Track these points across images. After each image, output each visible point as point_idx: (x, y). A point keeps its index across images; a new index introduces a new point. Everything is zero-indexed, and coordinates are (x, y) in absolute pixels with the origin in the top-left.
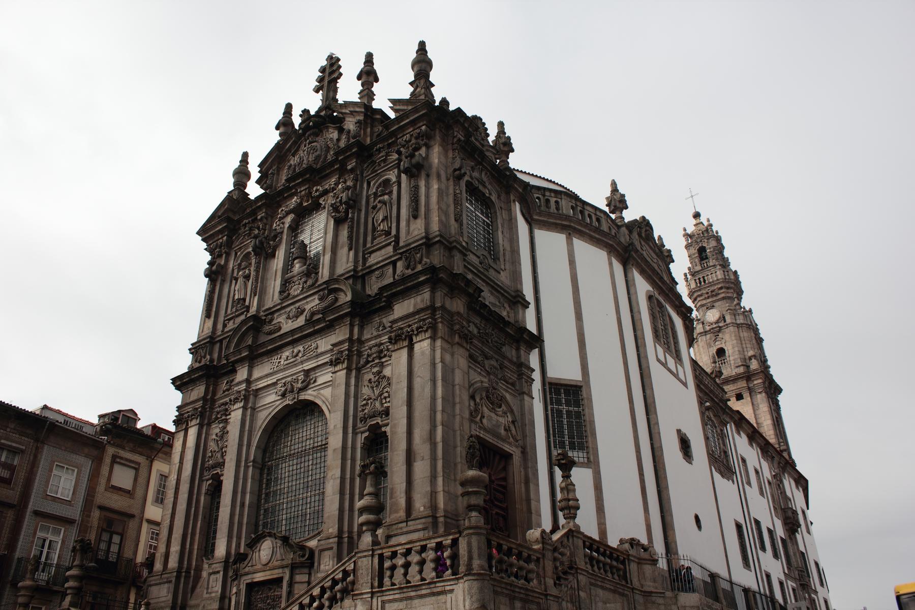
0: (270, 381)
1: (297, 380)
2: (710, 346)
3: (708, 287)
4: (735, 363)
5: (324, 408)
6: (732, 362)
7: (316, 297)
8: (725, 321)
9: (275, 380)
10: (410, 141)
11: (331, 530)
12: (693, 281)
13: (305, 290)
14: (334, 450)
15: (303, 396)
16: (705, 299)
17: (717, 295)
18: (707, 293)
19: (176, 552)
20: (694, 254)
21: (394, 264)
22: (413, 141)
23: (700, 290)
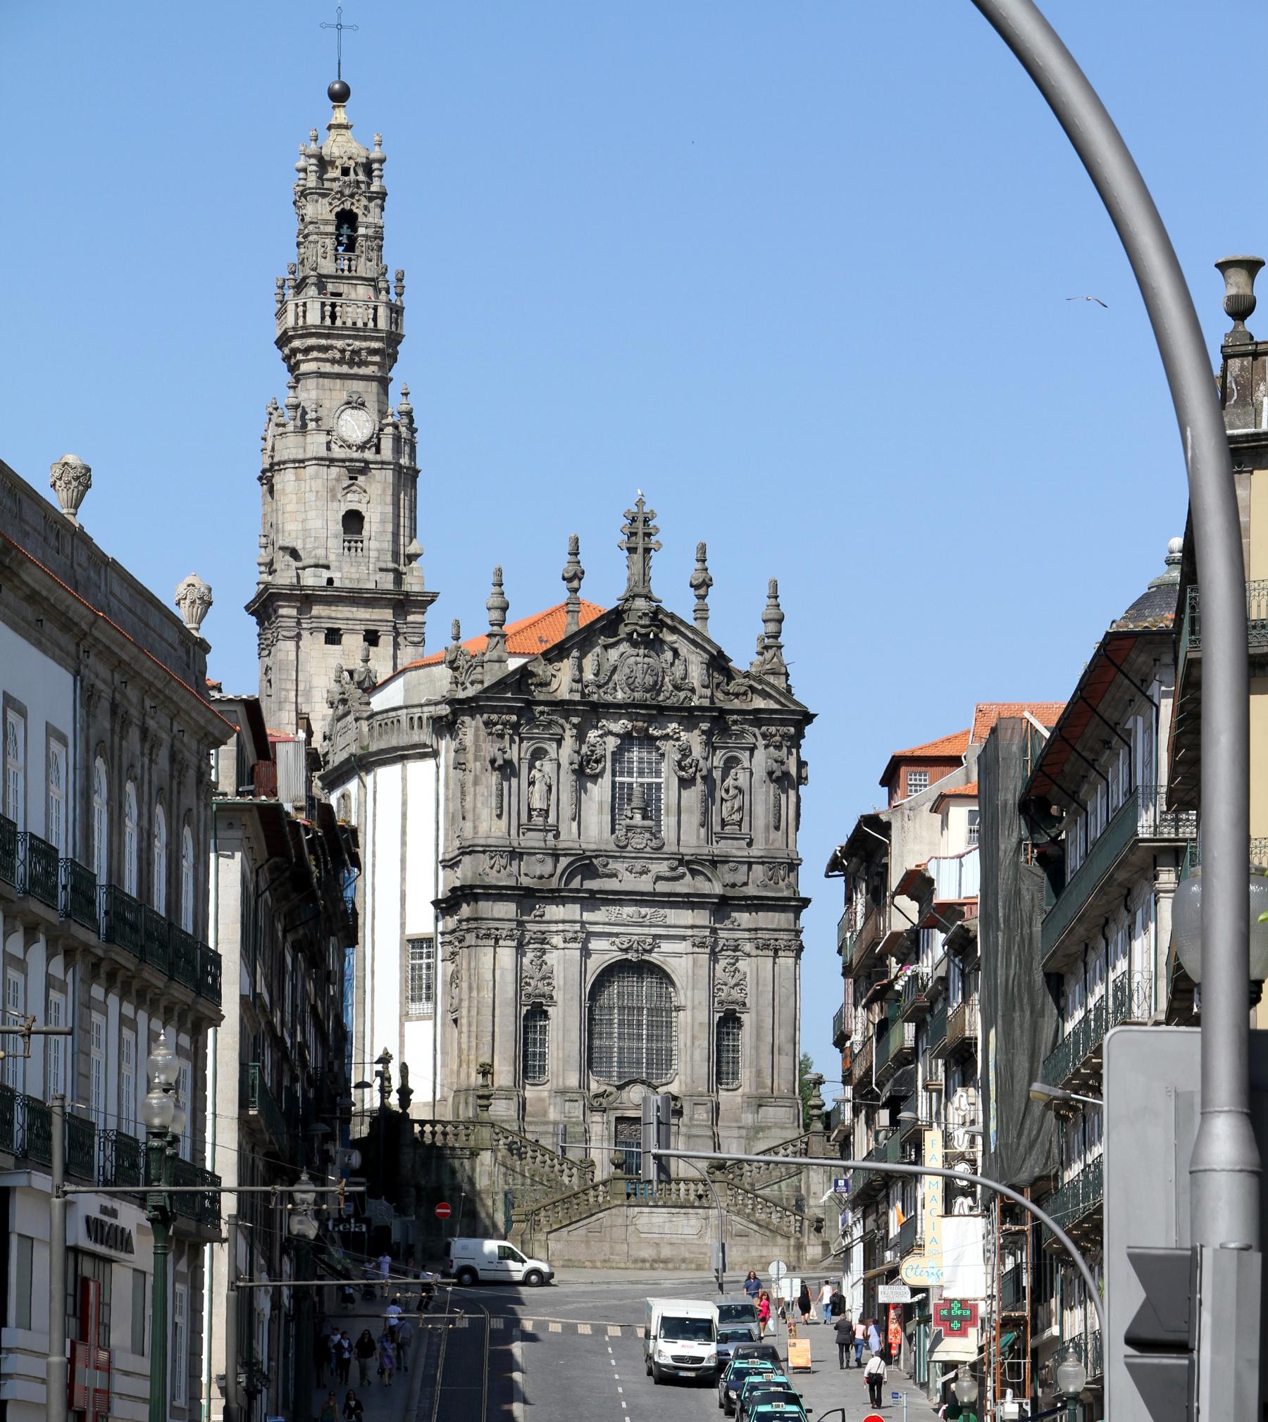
0: (607, 929)
1: (644, 942)
2: (334, 498)
3: (349, 337)
4: (378, 559)
5: (673, 976)
6: (373, 554)
7: (666, 862)
8: (378, 451)
9: (615, 931)
10: (775, 735)
11: (700, 1089)
12: (318, 306)
13: (648, 849)
14: (700, 1024)
15: (646, 957)
16: (333, 361)
17: (362, 363)
18: (343, 351)
19: (509, 1072)
20: (326, 222)
21: (750, 864)
22: (778, 738)
23: (328, 336)
